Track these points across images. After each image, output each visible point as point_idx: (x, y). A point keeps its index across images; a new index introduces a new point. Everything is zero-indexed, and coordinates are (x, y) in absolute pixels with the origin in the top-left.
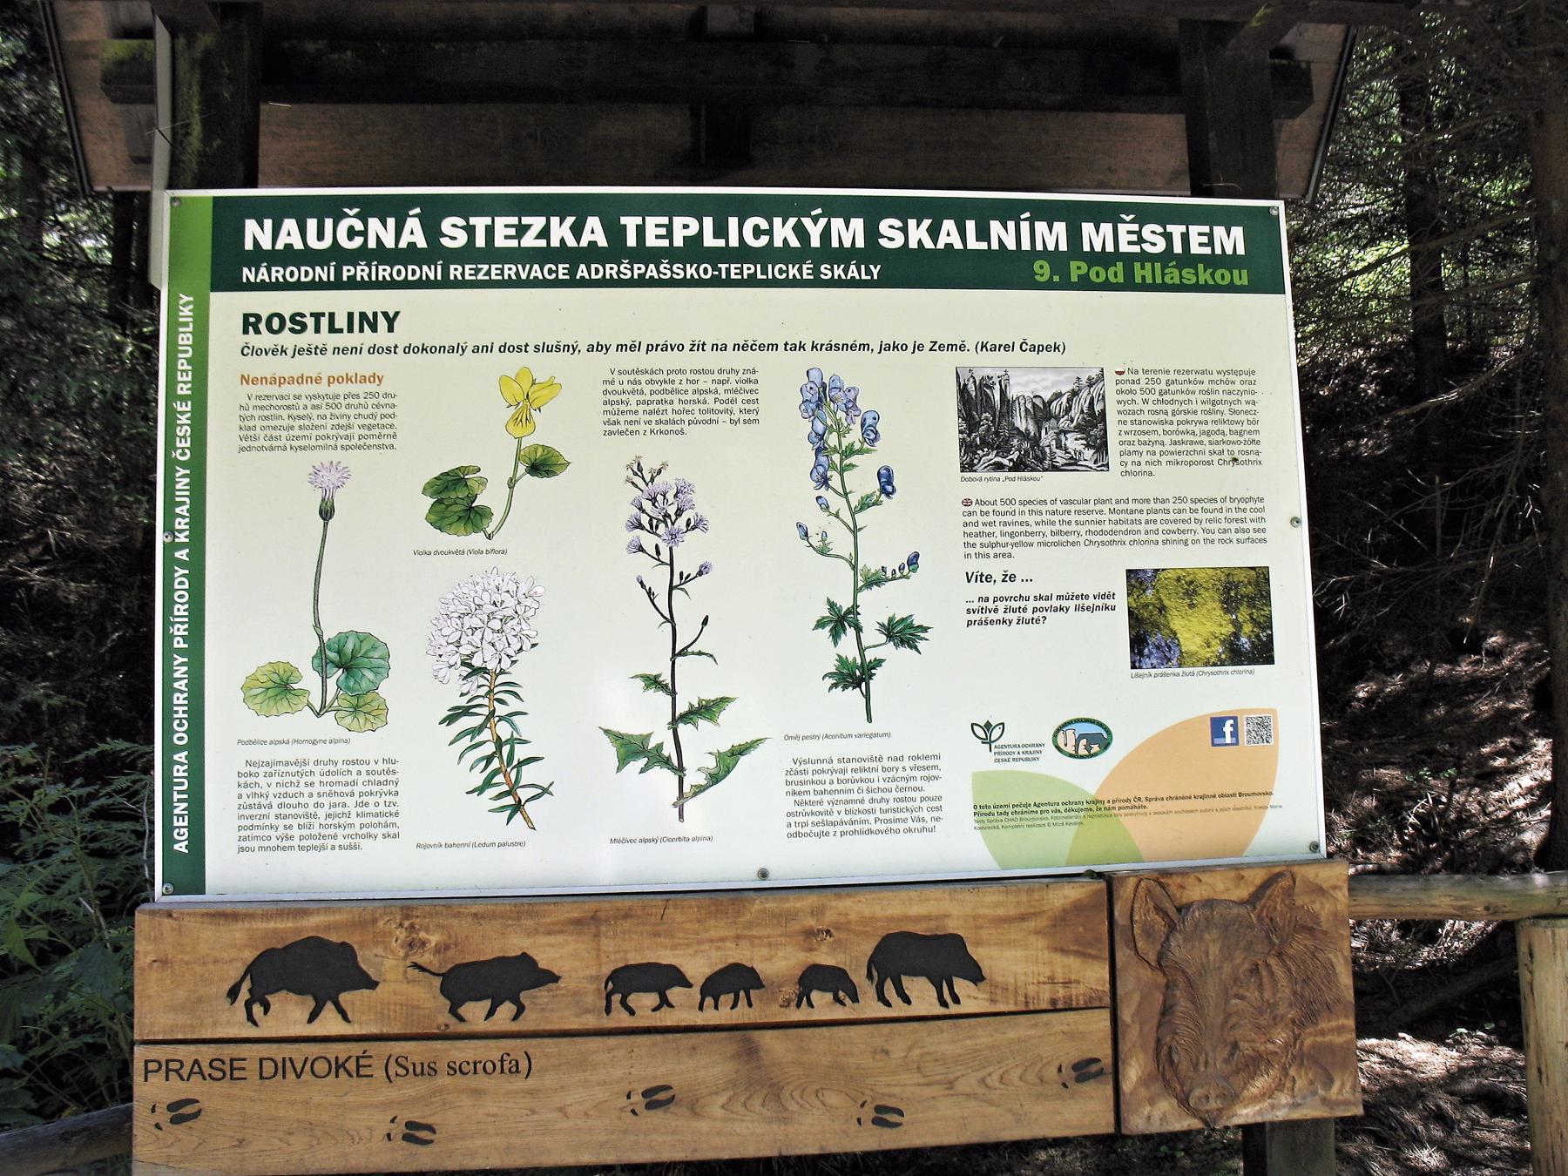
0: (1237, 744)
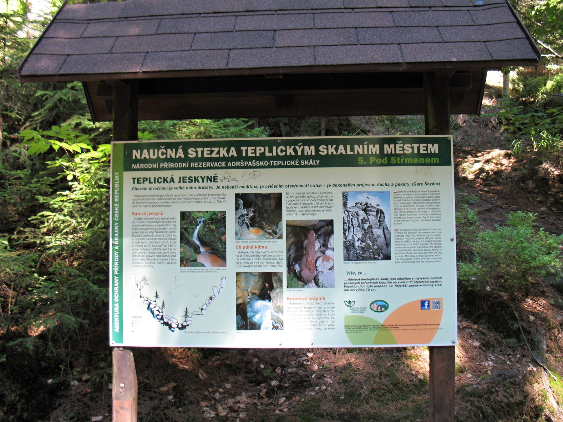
0: (429, 309)
